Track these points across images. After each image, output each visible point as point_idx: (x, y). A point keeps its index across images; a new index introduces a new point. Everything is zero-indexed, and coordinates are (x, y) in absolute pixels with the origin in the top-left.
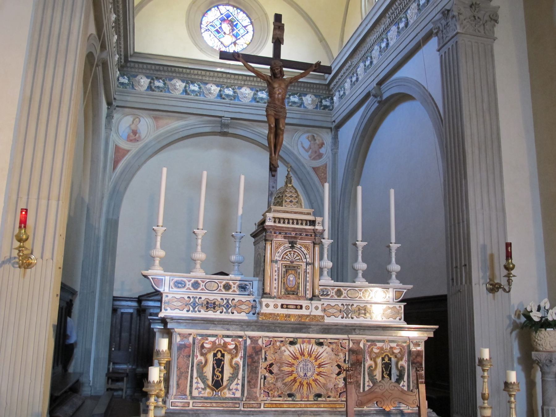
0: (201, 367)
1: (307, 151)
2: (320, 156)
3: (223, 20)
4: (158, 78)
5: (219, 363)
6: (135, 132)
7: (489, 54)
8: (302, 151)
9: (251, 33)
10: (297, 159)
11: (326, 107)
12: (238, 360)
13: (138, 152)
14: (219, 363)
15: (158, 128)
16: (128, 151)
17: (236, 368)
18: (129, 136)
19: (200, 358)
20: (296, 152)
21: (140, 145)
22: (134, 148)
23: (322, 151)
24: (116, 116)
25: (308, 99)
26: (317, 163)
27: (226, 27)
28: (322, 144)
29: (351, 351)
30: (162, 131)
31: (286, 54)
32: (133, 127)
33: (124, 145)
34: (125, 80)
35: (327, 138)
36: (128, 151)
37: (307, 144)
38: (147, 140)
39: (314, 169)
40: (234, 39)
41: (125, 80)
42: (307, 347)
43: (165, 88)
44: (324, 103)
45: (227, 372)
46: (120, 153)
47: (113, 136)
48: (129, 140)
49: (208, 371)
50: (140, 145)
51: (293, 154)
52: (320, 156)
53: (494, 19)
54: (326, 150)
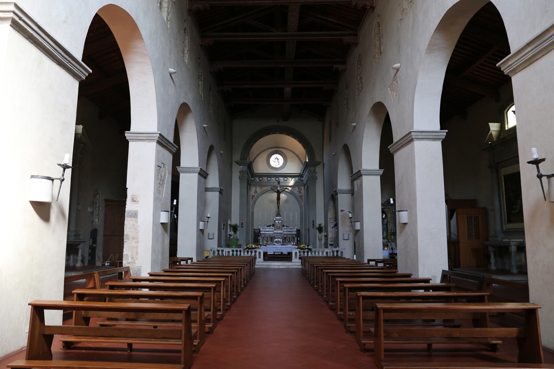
0: (265, 239)
1: (298, 192)
2: (301, 192)
3: (276, 158)
4: (260, 178)
5: (267, 239)
6: (256, 191)
7: (315, 186)
8: (296, 192)
9: (283, 161)
10: (295, 193)
11: (302, 180)
12: (270, 238)
13: (257, 196)
14: (267, 239)
15: (261, 189)
16: (255, 196)
17: (269, 239)
18: (255, 192)
19: (265, 238)
20: (295, 192)
21: (258, 194)
22: (256, 195)
23: (301, 191)
24: (251, 188)
25: (297, 179)
26: (301, 194)
27: (276, 160)
28: (302, 189)
29: (285, 237)
30: (262, 190)
31: (275, 195)
32: (256, 190)
33: (254, 194)
34: (253, 179)
35: (303, 188)
36: (255, 196)
37: (297, 190)
38: (259, 193)
39: (300, 196)
40: (278, 163)
41: (253, 179)
42: (278, 236)
43: (262, 180)
44: (301, 179)
45: (268, 240)
46: (253, 196)
47: (251, 192)
48: (255, 193)
49: (266, 239)
50: (258, 194)
51: (294, 193)
52: (301, 192)
53: (316, 179)
54: (303, 191)
